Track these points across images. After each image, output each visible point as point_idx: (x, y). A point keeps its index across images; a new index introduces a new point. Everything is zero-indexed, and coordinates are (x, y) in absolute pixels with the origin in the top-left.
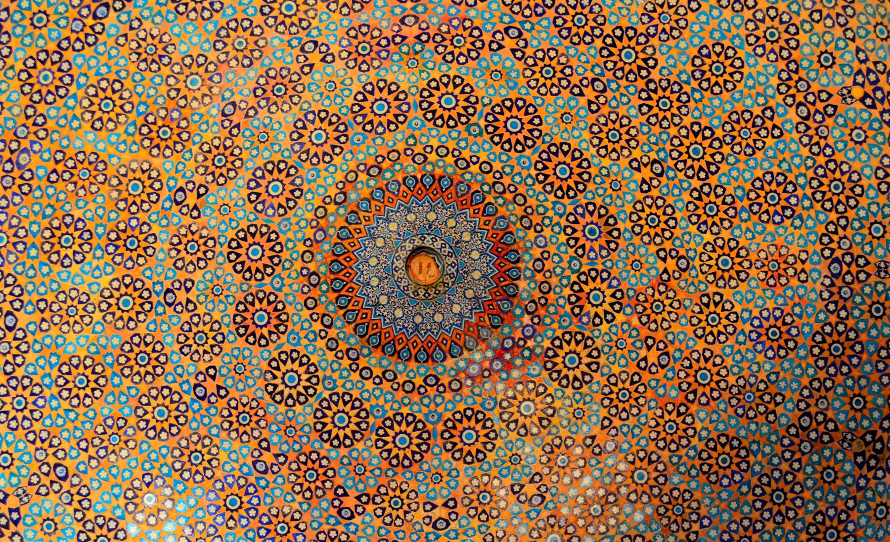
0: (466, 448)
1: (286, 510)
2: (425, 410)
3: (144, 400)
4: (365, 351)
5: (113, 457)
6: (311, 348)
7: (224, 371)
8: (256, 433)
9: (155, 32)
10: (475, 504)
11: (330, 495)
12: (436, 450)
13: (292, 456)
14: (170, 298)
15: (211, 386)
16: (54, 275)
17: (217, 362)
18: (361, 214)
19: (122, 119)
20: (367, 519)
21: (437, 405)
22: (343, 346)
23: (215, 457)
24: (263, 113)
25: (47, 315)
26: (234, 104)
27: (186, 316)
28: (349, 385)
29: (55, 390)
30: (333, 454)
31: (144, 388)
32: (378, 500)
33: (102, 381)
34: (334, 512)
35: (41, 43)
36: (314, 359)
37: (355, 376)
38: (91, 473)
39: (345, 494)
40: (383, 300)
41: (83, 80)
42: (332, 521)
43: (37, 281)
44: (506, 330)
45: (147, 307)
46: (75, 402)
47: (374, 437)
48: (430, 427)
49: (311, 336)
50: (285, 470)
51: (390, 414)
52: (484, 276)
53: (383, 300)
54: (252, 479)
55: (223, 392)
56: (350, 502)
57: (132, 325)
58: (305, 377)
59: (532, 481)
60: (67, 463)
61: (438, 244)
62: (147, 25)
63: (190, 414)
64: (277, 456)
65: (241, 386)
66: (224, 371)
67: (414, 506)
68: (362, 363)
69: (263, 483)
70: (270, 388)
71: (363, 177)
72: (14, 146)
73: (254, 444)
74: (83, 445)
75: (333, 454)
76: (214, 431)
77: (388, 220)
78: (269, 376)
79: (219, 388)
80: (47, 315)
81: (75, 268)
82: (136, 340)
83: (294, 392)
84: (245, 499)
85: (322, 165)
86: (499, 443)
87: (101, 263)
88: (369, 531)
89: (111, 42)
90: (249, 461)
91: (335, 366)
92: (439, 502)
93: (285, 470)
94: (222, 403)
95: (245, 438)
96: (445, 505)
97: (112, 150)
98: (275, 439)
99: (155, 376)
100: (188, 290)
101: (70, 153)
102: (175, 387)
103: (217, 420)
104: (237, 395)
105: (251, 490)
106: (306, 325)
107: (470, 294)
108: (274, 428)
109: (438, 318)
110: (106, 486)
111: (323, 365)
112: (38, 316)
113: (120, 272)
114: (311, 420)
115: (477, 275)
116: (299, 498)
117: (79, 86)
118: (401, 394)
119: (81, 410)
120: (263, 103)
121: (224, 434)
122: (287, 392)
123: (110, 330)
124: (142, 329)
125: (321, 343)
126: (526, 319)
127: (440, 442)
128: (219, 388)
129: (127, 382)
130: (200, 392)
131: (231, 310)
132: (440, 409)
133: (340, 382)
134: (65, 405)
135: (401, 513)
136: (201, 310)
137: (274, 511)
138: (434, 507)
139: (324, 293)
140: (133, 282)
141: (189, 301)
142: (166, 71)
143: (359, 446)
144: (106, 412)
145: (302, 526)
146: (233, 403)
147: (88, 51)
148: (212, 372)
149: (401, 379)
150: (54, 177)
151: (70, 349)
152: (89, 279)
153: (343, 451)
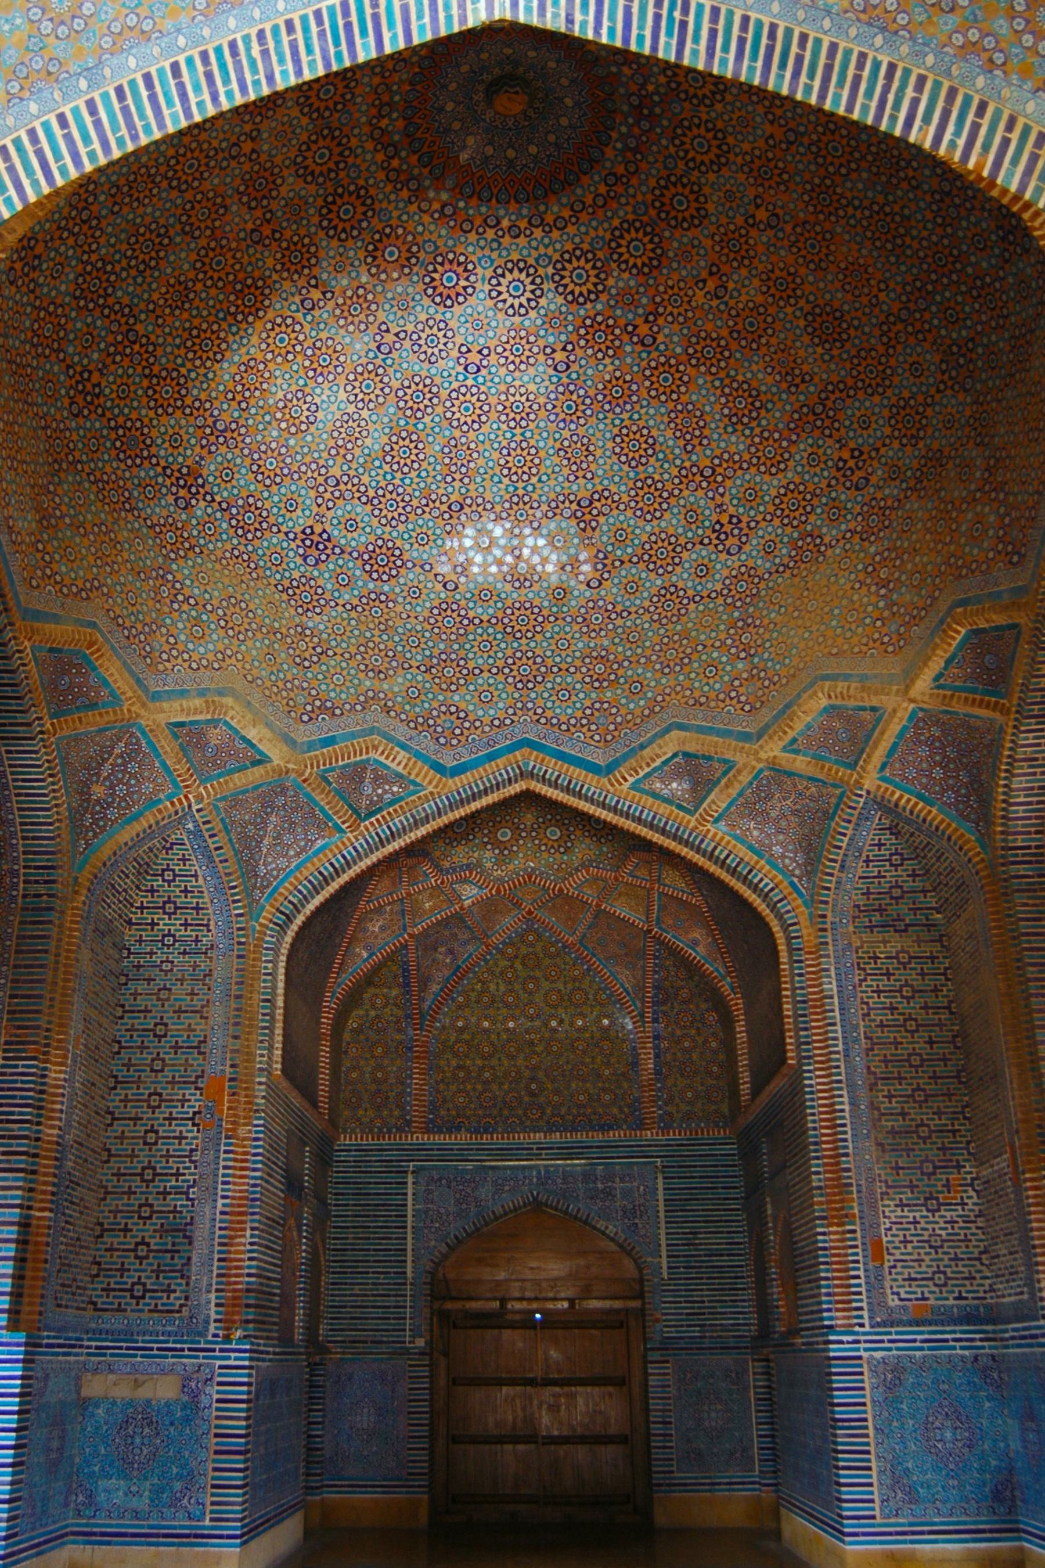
0: (687, 214)
1: (607, 377)
2: (629, 209)
3: (449, 415)
4: (542, 208)
5: (472, 465)
6: (504, 253)
7: (470, 339)
8: (535, 350)
9: (164, 290)
10: (732, 256)
11: (626, 338)
12: (667, 234)
13: (574, 338)
14: (385, 349)
15: (474, 357)
16: (317, 433)
17: (459, 340)
18: (419, 135)
19: (222, 335)
20: (666, 331)
21: (634, 196)
22: (523, 224)
23: (528, 393)
24: (274, 205)
25: (342, 451)
26: (253, 231)
27: (407, 344)
28: (558, 246)
29: (399, 475)
30: (599, 307)
31: (439, 410)
32: (661, 310)
33: (414, 437)
34: (639, 348)
35: (140, 392)
36: (515, 256)
37: (556, 234)
38: (472, 487)
39: (635, 327)
40: (511, 153)
41: (179, 361)
42: (644, 355)
43: (314, 447)
44: (622, 91)
45: (381, 371)
46: (416, 466)
47: (614, 265)
48: (645, 219)
49: (495, 245)
50: (579, 352)
51: (608, 236)
52: (558, 61)
53: (511, 153)
54: (565, 380)
55: (485, 352)
56: (644, 329)
57: (387, 390)
58: (523, 276)
59: (758, 207)
60: (453, 498)
61: (497, 71)
62: (155, 296)
63: (483, 388)
64: (564, 349)
65: (491, 334)
66: (470, 339)
67: (690, 293)
68: (549, 219)
69: (574, 376)
70: (511, 311)
71: (384, 123)
72: (208, 431)
73: (541, 358)
74: (449, 479)
75: (599, 307)
76: (509, 379)
77: (441, 110)
78: (500, 305)
79: (480, 352)
80: (342, 451)
81: (320, 415)
82: (400, 393)
83: (528, 295)
84: (574, 397)
85: (350, 160)
86: (707, 190)
87: (327, 392)
88: (676, 339)
89: (159, 332)
90: (551, 372)
91: (534, 244)
92: (704, 274)
93: (579, 352)
94: (493, 357)
95: (532, 361)
96: (711, 274)
97: (244, 350)
98: (551, 339)
99: (436, 395)
100: (388, 331)
101: (231, 385)
102: (455, 385)
103: (503, 371)
104: (495, 342)
105: (572, 388)
106: (482, 243)
107: (564, 81)
108: (542, 333)
109: (564, 122)
110: (488, 484)
111: (525, 252)
112: (340, 460)
113: (341, 380)
114: (560, 300)
115: (552, 64)
116: (607, 361)
117: (183, 365)
118: (600, 213)
119: (424, 465)
120: (265, 202)
121: (517, 374)
122: (523, 300)
123: (381, 411)
124: (396, 384)
125: (506, 240)
126: (626, 70)
127: (663, 225)
128: (480, 352)
129: (427, 419)
130: (472, 369)
131: (427, 301)
132: (640, 198)
133: (550, 251)
134: (413, 474)
135: (686, 306)
136: (410, 328)
137: (600, 386)
138: (704, 281)
139: (466, 208)
140: (355, 373)
141: (397, 335)
142: (199, 286)
143: (611, 282)
144: (437, 448)
145: (628, 378)
146: (500, 350)
147: (159, 352)
148: (464, 349)
149: (589, 200)
150: (244, 405)
151: (376, 447)
152: (333, 408)
153: (603, 298)
